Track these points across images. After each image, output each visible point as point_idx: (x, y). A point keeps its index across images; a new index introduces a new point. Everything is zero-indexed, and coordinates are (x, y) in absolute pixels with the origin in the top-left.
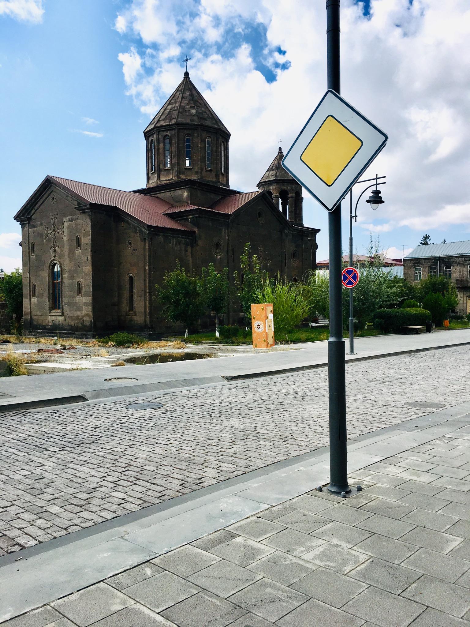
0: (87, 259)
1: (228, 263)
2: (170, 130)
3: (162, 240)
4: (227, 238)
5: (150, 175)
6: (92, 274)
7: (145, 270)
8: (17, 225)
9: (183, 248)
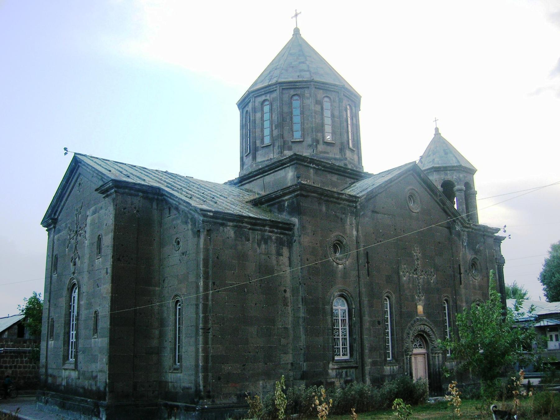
0: (107, 273)
1: (359, 277)
2: (271, 92)
3: (232, 233)
4: (355, 233)
5: (245, 158)
6: (112, 297)
7: (198, 287)
8: (44, 231)
9: (273, 248)
